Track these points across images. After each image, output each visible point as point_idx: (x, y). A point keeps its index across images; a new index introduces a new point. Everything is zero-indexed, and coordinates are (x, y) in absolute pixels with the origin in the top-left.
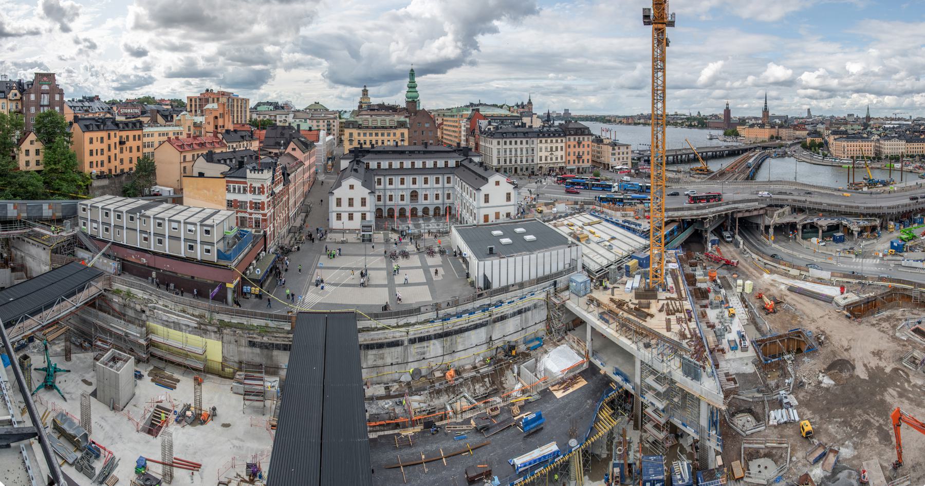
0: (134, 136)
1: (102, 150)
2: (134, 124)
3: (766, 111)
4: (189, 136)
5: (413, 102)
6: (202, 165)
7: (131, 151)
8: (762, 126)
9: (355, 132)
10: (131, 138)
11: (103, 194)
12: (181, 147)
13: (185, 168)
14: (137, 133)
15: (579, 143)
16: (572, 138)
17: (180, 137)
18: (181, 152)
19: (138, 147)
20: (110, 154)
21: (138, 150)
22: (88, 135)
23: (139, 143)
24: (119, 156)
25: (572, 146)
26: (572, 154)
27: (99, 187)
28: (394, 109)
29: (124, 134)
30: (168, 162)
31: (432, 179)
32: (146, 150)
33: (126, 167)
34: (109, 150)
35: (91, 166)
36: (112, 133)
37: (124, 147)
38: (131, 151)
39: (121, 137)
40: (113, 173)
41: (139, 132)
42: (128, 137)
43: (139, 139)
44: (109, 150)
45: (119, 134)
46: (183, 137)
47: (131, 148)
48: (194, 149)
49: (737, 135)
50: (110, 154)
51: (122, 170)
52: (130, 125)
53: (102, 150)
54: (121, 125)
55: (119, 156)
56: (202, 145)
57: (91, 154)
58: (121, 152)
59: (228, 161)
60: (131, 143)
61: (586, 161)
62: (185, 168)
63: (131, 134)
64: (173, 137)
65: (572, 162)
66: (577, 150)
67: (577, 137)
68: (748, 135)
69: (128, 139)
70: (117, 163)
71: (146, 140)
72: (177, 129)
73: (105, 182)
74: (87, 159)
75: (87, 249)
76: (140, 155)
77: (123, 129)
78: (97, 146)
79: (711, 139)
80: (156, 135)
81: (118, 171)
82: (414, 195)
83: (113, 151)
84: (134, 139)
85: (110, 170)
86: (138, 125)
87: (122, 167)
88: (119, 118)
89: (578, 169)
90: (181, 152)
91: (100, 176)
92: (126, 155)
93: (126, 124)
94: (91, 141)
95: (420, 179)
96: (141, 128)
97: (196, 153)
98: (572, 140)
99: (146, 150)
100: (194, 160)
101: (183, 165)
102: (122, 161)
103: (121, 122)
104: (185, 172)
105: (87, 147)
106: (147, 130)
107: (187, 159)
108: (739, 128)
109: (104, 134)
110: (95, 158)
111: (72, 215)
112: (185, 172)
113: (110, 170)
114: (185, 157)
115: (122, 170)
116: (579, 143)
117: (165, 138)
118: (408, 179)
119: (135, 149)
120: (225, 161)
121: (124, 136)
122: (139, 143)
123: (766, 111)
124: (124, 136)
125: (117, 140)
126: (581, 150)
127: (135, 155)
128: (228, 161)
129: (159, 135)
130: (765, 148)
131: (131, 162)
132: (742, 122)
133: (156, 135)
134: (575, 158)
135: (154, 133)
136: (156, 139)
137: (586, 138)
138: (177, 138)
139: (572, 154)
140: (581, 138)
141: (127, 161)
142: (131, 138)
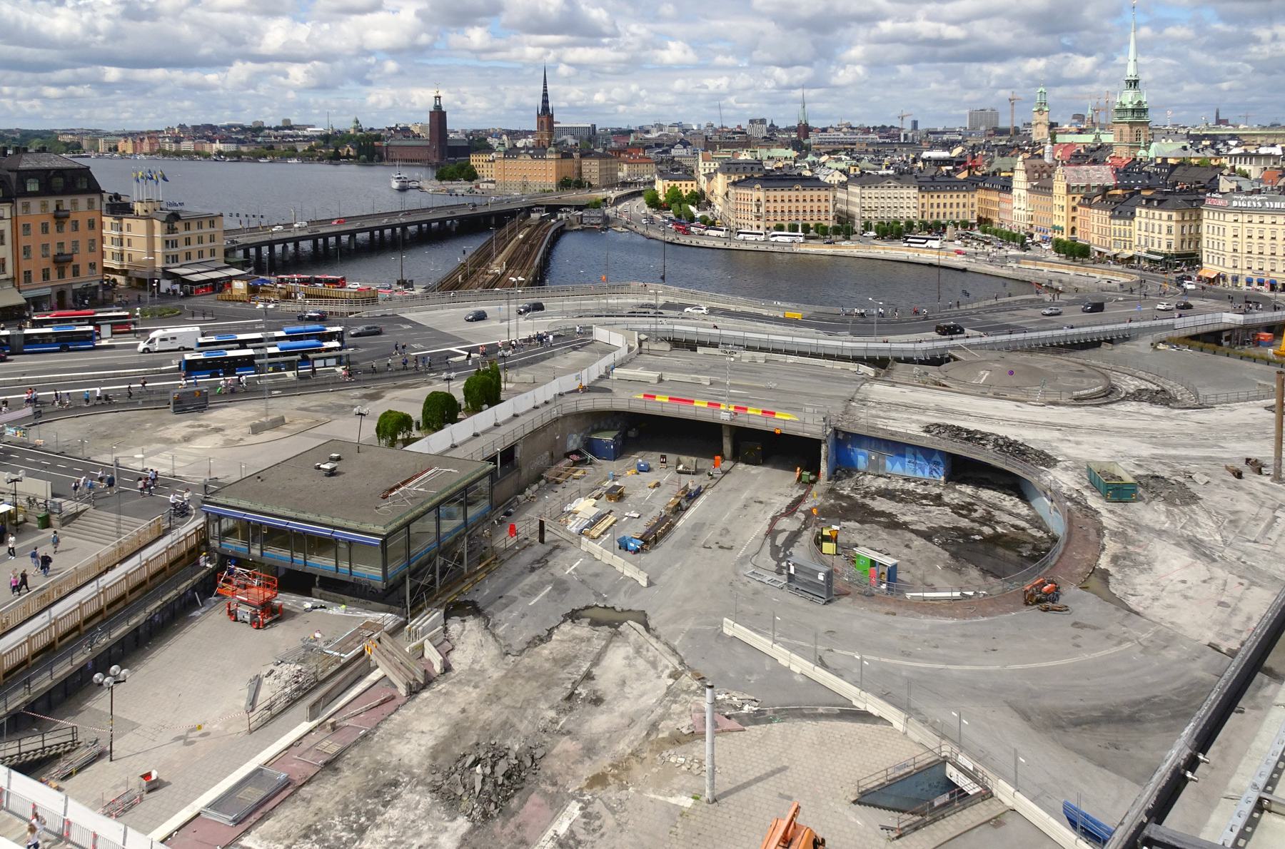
3: (546, 113)
8: (538, 151)
15: (60, 217)
16: (35, 204)
25: (36, 228)
26: (36, 252)
49: (472, 176)
61: (84, 270)
65: (37, 277)
66: (53, 237)
67: (52, 202)
68: (502, 181)
79: (403, 189)
89: (61, 294)
98: (38, 210)
108: (476, 160)
116: (60, 217)
123: (546, 113)
126: (68, 237)
130: (553, 209)
132: (478, 143)
134: (47, 263)
137: (82, 201)
139: (36, 252)
140: (67, 202)
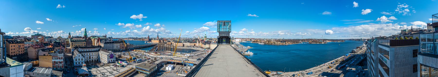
5: (86, 36)
6: (41, 53)
9: (73, 43)
14: (23, 44)
22: (11, 45)
28: (81, 37)
29: (20, 44)
30: (32, 52)
31: (94, 53)
60: (22, 47)
63: (21, 44)
78: (13, 48)
82: (90, 57)
93: (20, 42)
95: (91, 53)
105: (11, 48)
110: (13, 51)
118: (88, 53)
127: (22, 50)
135: (27, 44)
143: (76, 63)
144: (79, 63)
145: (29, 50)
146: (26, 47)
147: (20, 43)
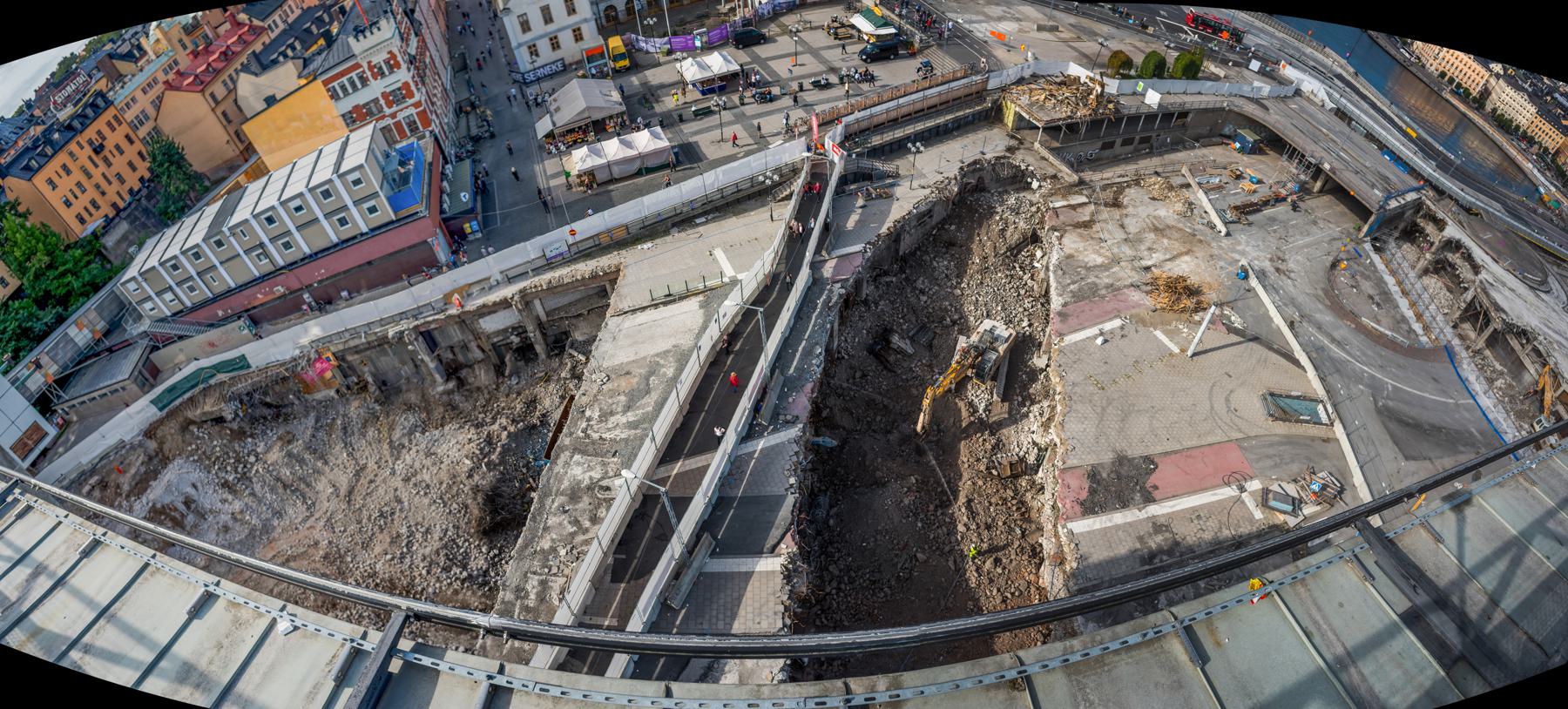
0: (109, 124)
1: (79, 184)
2: (94, 105)
4: (195, 54)
6: (249, 88)
7: (122, 152)
10: (106, 131)
11: (141, 245)
12: (200, 84)
13: (224, 114)
14: (108, 115)
17: (182, 67)
18: (202, 91)
19: (127, 137)
20: (94, 181)
21: (131, 142)
23: (124, 129)
24: (111, 173)
27: (119, 242)
29: (90, 133)
30: (191, 120)
32: (143, 132)
33: (133, 181)
34: (89, 176)
35: (82, 221)
36: (73, 146)
37: (106, 152)
38: (122, 152)
39: (90, 142)
40: (122, 205)
41: (111, 112)
42: (99, 133)
43: (120, 124)
44: (89, 176)
45: (83, 138)
46: (185, 62)
47: (118, 147)
48: (218, 72)
50: (94, 181)
51: (131, 191)
52: (89, 111)
53: (79, 184)
54: (76, 124)
55: (111, 173)
56: (227, 56)
57: (68, 204)
58: (109, 164)
59: (289, 52)
60: (114, 138)
62: (224, 114)
63: (100, 124)
64: (171, 76)
69: (104, 138)
70: (116, 185)
71: (130, 115)
72: (164, 59)
73: (124, 227)
74: (69, 216)
75: (181, 338)
76: (138, 146)
77: (85, 126)
78: (66, 184)
80: (139, 94)
81: (128, 198)
83: (97, 173)
84: (113, 129)
85: (114, 205)
86: (100, 101)
87: (127, 186)
88: (63, 115)
90: (202, 91)
91: (109, 224)
92: (119, 164)
93: (82, 116)
94: (50, 182)
96: (109, 103)
97: (225, 77)
99: (143, 132)
100: (232, 91)
101: (219, 112)
102: (121, 180)
103: (73, 117)
104: (229, 122)
105: (55, 198)
106: (120, 95)
107: (219, 98)
109: (62, 158)
110: (79, 206)
111: (121, 312)
112: (229, 122)
113: (114, 205)
114: (213, 96)
115: (131, 191)
117: (159, 88)
119: (124, 144)
120: (286, 56)
121: (94, 136)
122: (124, 129)
124: (94, 136)
125: (88, 150)
127: (131, 152)
128: (289, 52)
129: (144, 91)
131: (134, 169)
133: (139, 94)
136: (144, 102)
138: (178, 72)
141: (129, 169)
142: (106, 131)
143: (533, 51)
144: (555, 45)
145: (168, 126)
146: (141, 120)
147: (84, 119)
